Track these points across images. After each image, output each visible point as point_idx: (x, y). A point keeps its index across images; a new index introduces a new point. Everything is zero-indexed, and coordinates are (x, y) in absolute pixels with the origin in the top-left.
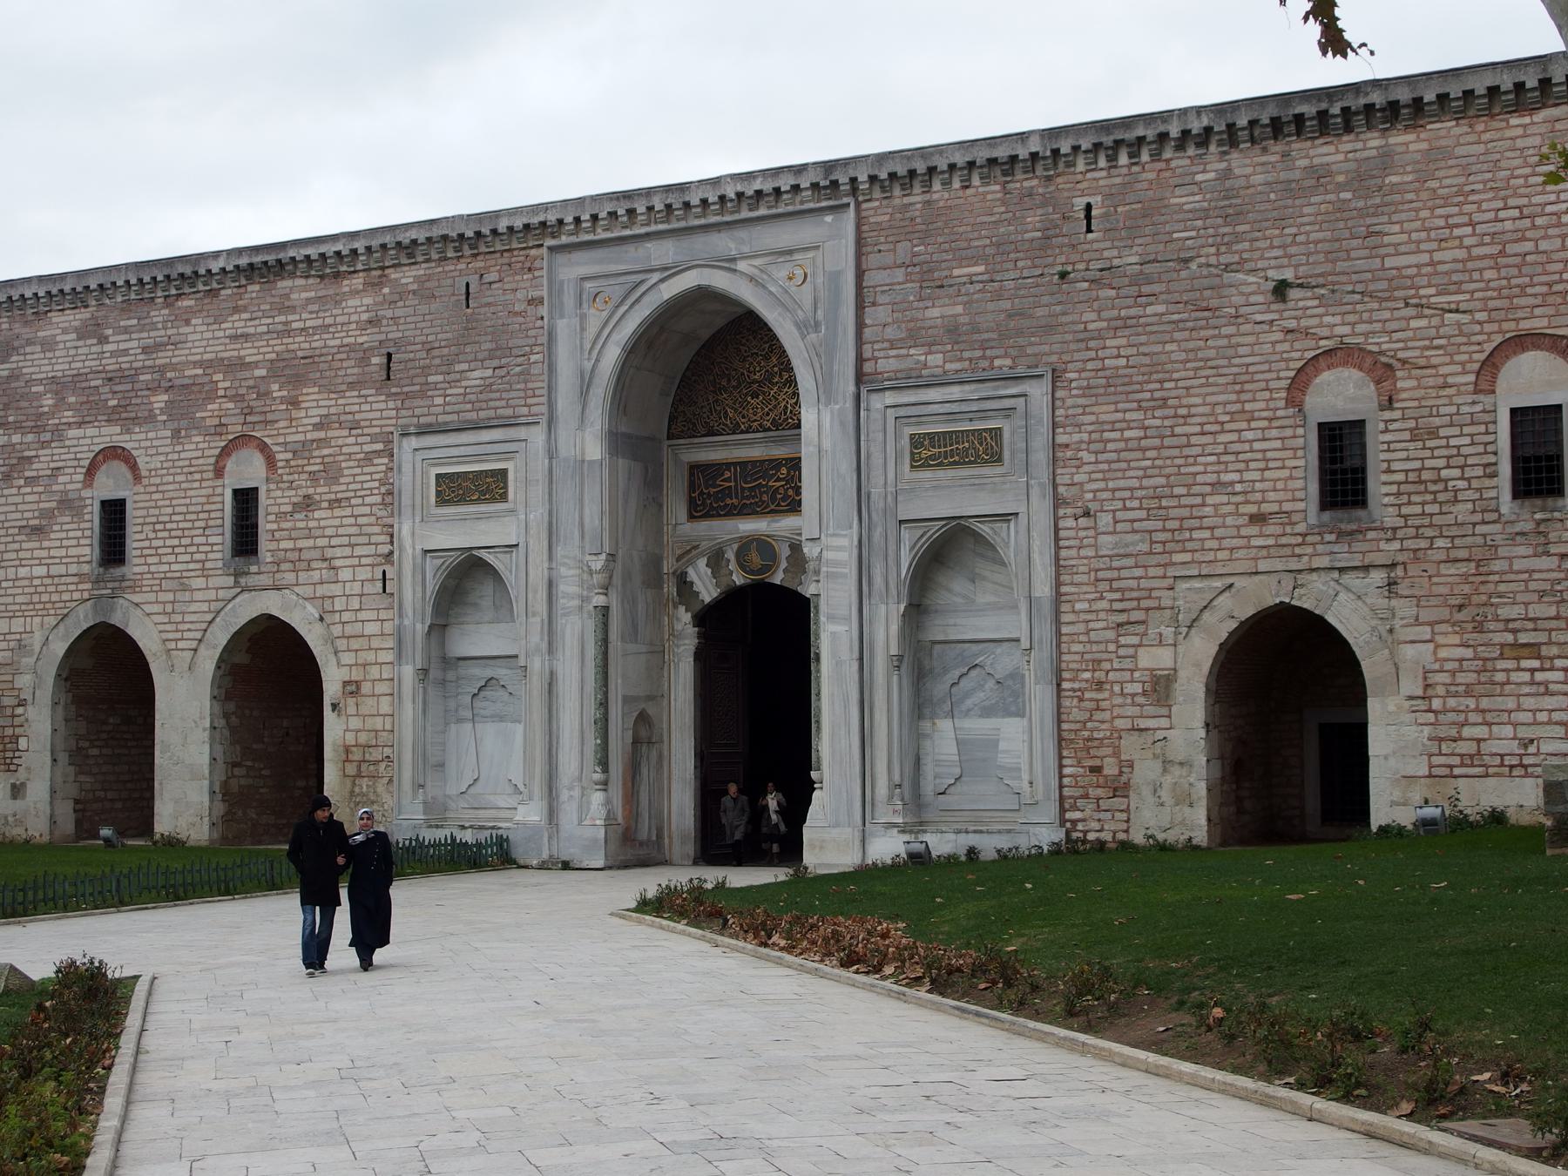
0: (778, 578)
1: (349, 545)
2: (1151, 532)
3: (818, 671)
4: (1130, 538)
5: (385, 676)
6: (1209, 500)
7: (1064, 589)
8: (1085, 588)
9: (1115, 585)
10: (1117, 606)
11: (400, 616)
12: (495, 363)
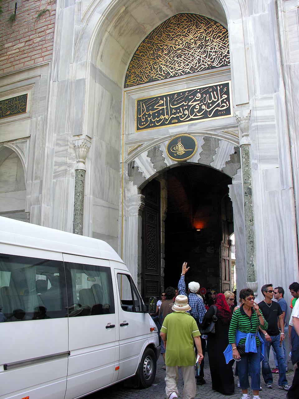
0: (195, 159)
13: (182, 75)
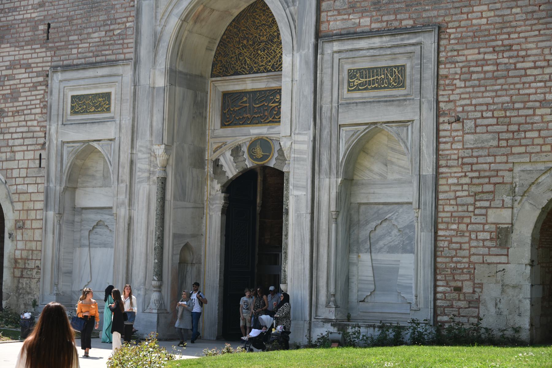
1: (23, 138)
2: (499, 133)
3: (287, 220)
4: (485, 136)
5: (38, 217)
6: (538, 112)
7: (441, 170)
8: (455, 170)
9: (474, 167)
10: (475, 181)
11: (48, 181)
12: (107, 28)
13: (264, 72)
